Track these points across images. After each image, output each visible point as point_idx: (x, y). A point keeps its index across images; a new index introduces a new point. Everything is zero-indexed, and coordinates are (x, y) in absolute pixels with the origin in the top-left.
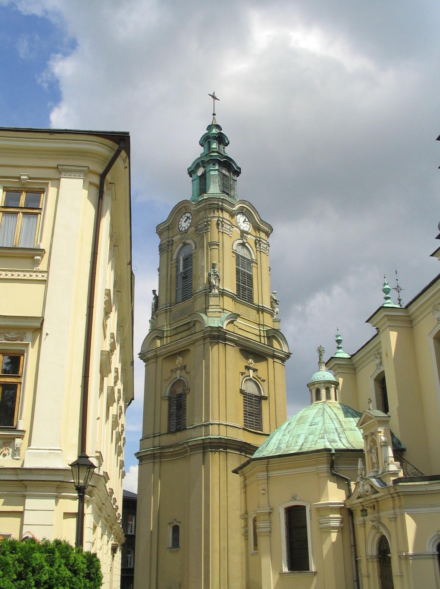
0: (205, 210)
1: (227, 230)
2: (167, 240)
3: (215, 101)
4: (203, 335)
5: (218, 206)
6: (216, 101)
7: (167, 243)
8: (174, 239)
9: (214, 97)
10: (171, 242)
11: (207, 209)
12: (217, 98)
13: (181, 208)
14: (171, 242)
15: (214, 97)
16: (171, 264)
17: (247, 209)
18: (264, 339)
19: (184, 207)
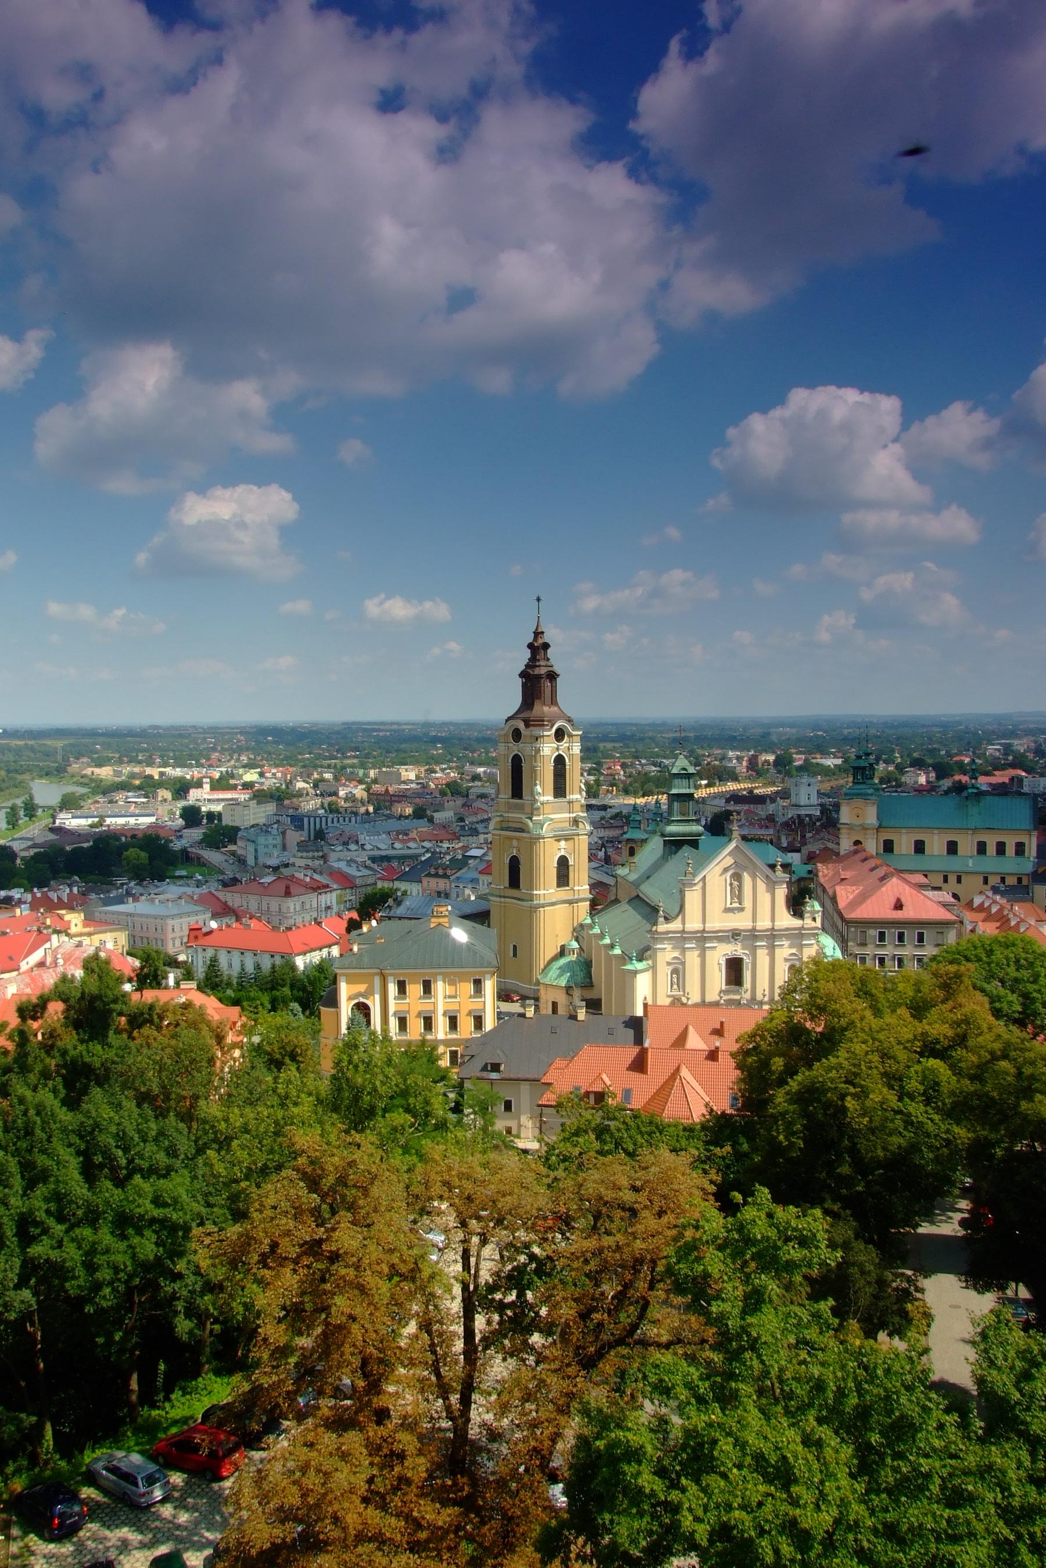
9: (538, 600)
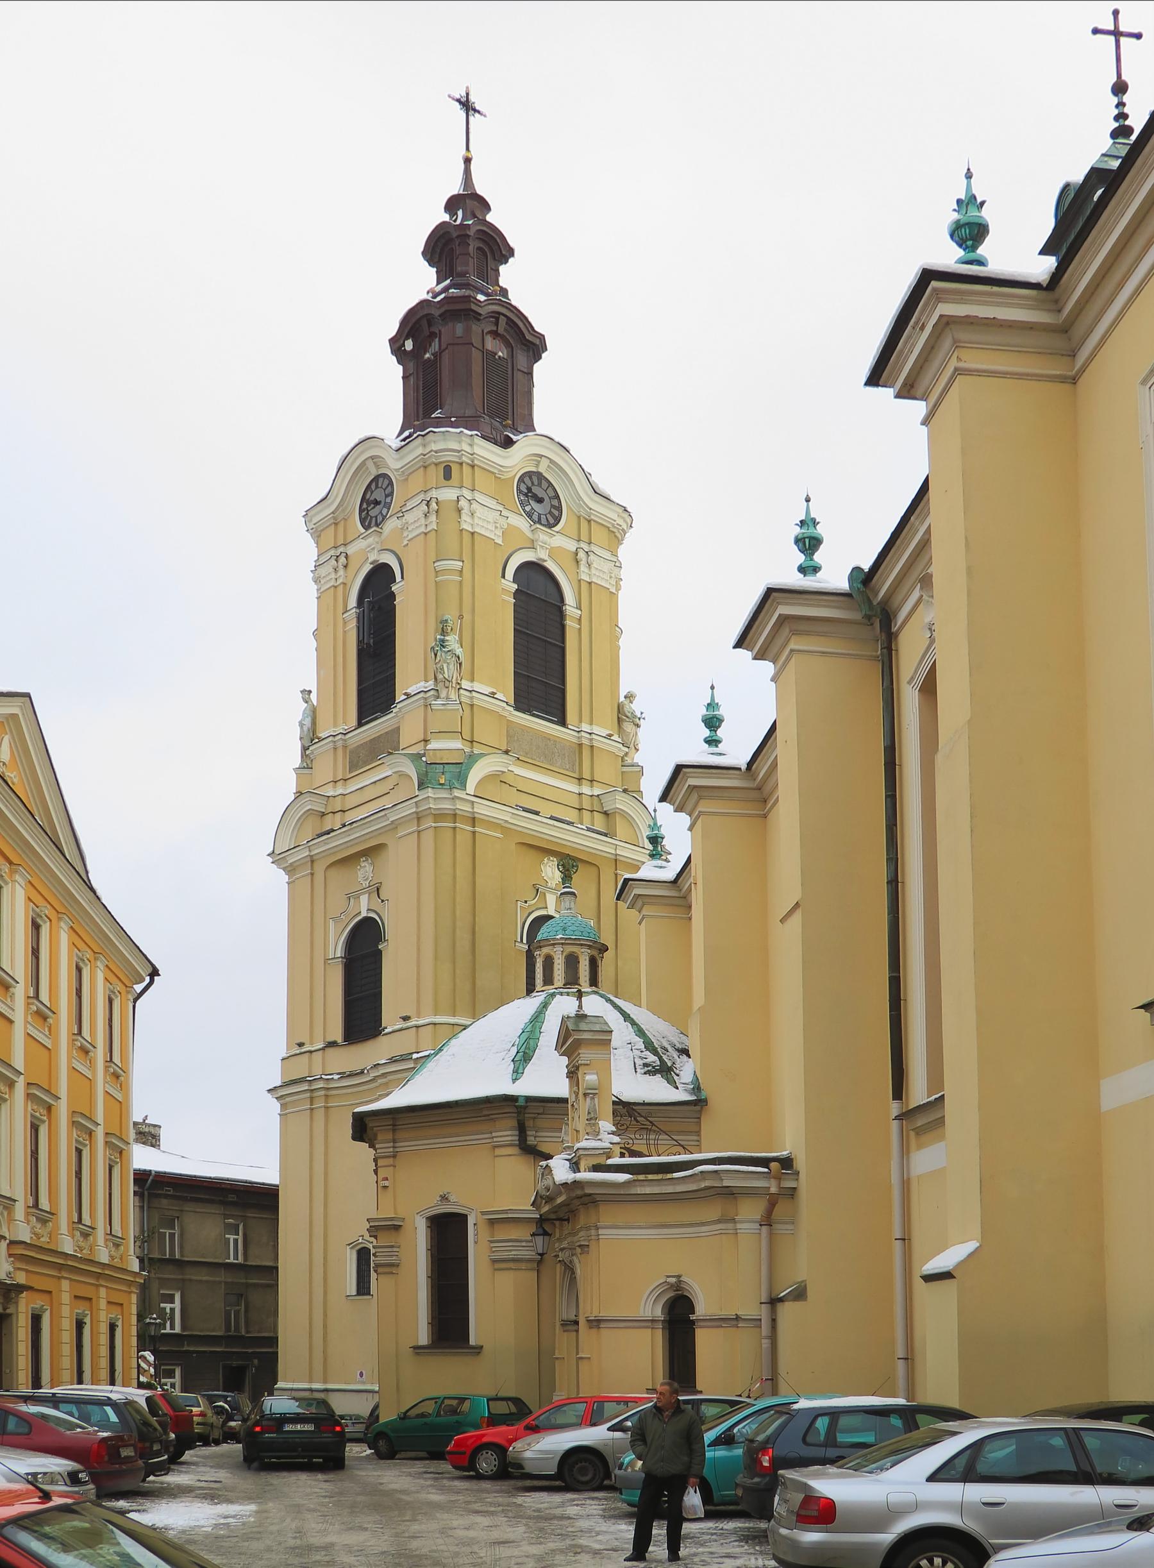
0: (425, 467)
1: (485, 525)
2: (332, 552)
3: (471, 118)
4: (414, 810)
5: (460, 457)
6: (475, 119)
7: (333, 562)
8: (351, 550)
9: (467, 105)
10: (342, 559)
11: (429, 465)
12: (477, 108)
13: (363, 463)
14: (342, 559)
15: (467, 105)
16: (345, 623)
17: (551, 461)
18: (593, 818)
19: (372, 458)
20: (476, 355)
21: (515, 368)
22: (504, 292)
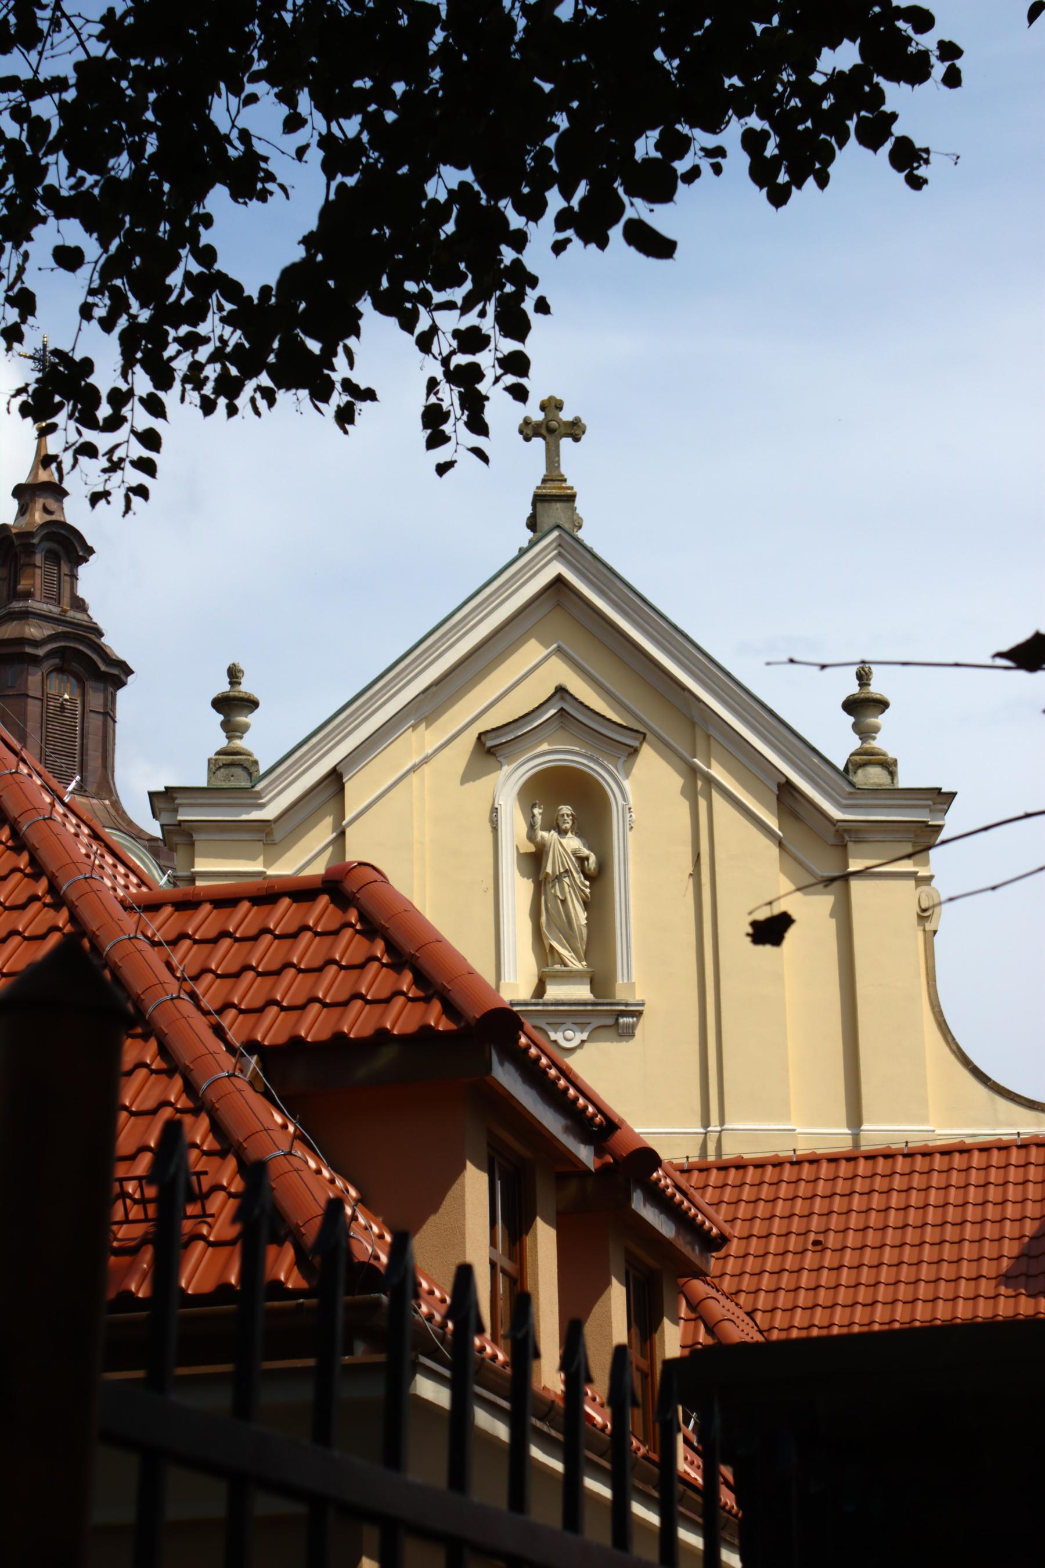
20: (33, 708)
21: (87, 709)
22: (80, 605)
